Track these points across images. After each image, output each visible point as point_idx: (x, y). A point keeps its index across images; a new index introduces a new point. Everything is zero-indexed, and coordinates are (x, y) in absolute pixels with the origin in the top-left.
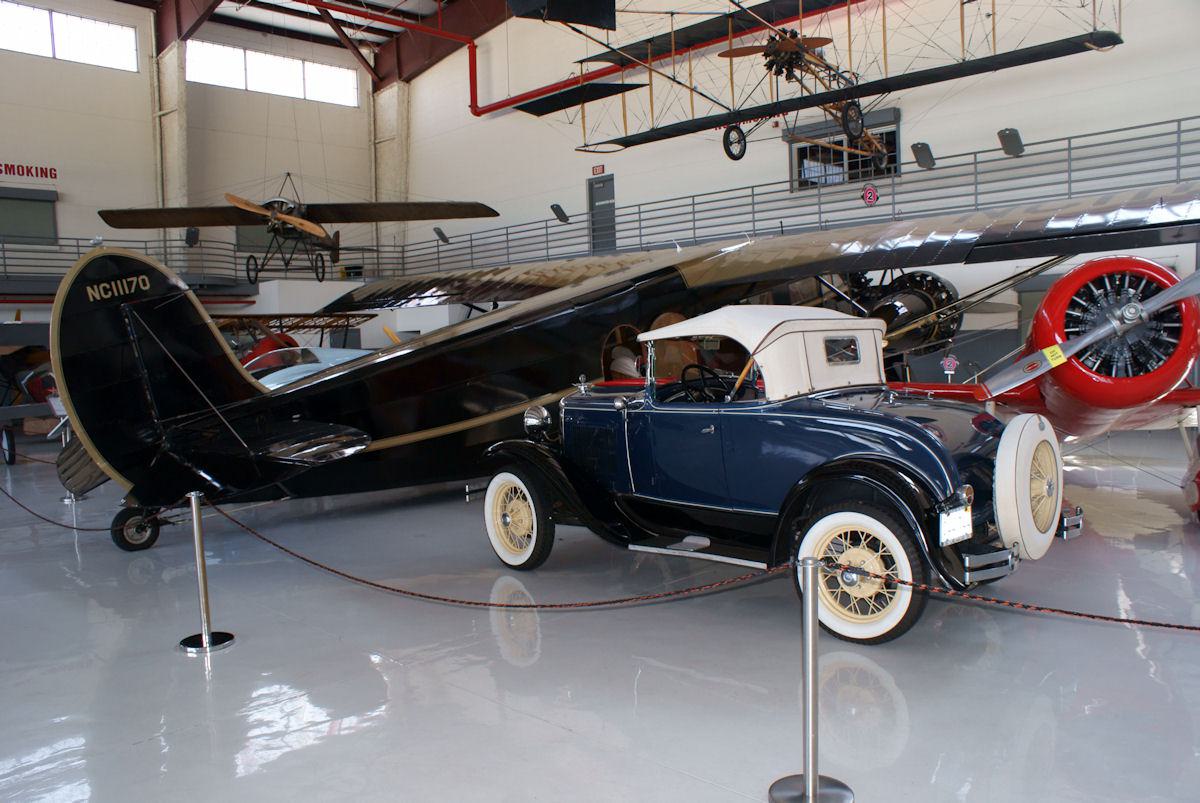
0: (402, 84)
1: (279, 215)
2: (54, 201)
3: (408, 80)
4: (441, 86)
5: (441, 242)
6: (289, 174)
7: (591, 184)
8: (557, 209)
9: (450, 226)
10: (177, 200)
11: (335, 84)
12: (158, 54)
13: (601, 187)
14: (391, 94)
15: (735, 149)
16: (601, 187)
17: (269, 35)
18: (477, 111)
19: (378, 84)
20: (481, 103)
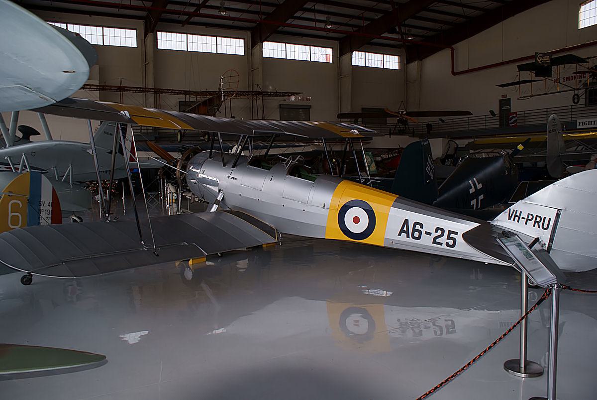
0: (420, 62)
1: (403, 116)
2: (309, 109)
3: (421, 60)
4: (436, 65)
5: (440, 122)
6: (402, 102)
7: (500, 101)
8: (492, 112)
9: (443, 118)
10: (347, 110)
11: (392, 62)
12: (340, 57)
13: (505, 102)
14: (414, 65)
15: (576, 101)
16: (505, 102)
17: (373, 46)
18: (454, 73)
19: (408, 62)
20: (455, 71)
